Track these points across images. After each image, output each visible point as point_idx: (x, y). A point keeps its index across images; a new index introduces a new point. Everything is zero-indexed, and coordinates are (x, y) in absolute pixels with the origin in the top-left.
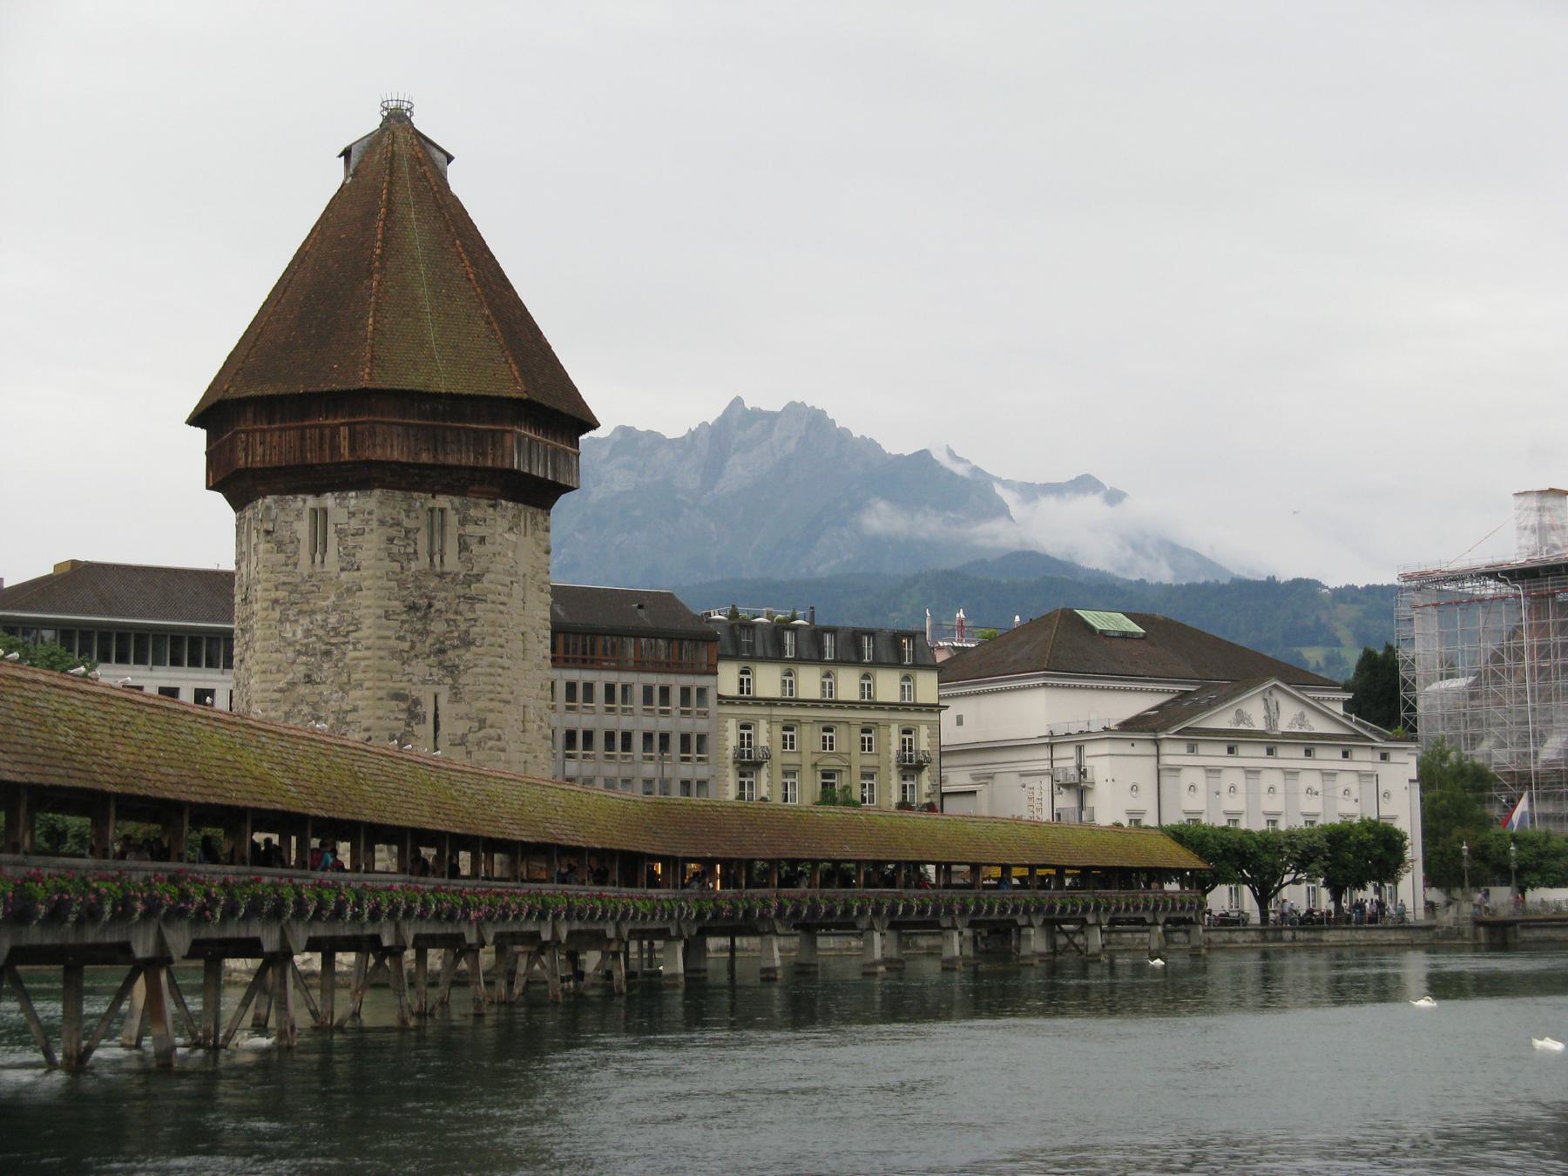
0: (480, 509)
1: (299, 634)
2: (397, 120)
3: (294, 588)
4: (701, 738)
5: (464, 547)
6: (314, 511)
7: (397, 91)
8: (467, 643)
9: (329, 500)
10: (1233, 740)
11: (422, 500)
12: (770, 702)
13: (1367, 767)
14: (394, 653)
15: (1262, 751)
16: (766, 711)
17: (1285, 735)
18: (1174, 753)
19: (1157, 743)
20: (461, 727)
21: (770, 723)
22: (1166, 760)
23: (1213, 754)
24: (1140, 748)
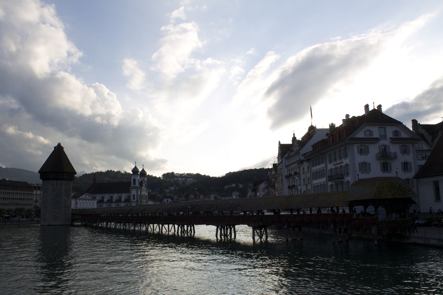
1: (55, 194)
2: (59, 144)
4: (32, 199)
5: (70, 186)
6: (57, 182)
7: (59, 142)
9: (58, 181)
10: (83, 199)
12: (39, 195)
13: (93, 202)
15: (85, 201)
16: (38, 196)
17: (87, 199)
18: (78, 201)
19: (76, 200)
21: (38, 197)
23: (81, 201)
24: (74, 200)
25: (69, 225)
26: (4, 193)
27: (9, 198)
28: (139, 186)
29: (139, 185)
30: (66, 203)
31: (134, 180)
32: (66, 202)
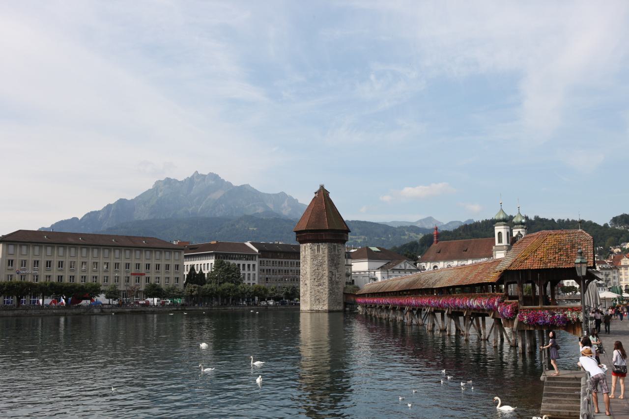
0: (340, 245)
2: (322, 187)
3: (315, 256)
5: (338, 251)
7: (322, 183)
8: (339, 264)
9: (320, 244)
10: (400, 270)
11: (333, 244)
14: (330, 266)
15: (404, 273)
18: (391, 273)
19: (388, 271)
20: (338, 276)
22: (389, 274)
23: (396, 273)
24: (385, 272)
25: (338, 311)
26: (273, 264)
27: (281, 271)
28: (509, 245)
29: (508, 242)
30: (334, 276)
31: (500, 233)
32: (333, 275)
